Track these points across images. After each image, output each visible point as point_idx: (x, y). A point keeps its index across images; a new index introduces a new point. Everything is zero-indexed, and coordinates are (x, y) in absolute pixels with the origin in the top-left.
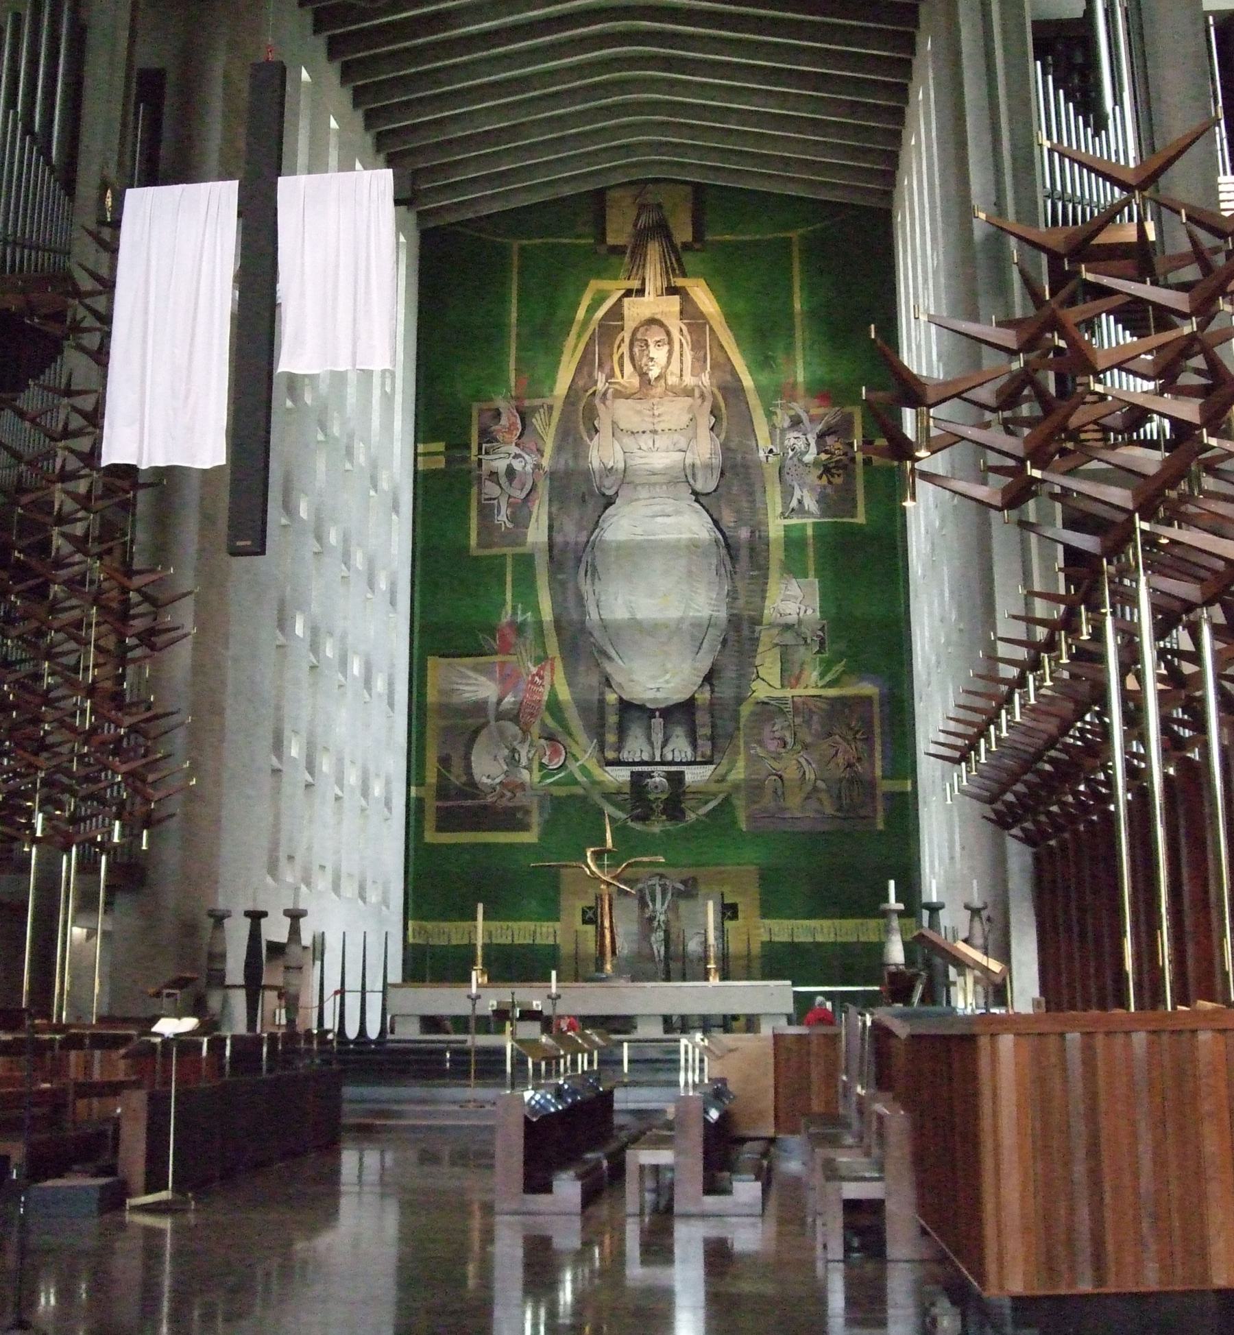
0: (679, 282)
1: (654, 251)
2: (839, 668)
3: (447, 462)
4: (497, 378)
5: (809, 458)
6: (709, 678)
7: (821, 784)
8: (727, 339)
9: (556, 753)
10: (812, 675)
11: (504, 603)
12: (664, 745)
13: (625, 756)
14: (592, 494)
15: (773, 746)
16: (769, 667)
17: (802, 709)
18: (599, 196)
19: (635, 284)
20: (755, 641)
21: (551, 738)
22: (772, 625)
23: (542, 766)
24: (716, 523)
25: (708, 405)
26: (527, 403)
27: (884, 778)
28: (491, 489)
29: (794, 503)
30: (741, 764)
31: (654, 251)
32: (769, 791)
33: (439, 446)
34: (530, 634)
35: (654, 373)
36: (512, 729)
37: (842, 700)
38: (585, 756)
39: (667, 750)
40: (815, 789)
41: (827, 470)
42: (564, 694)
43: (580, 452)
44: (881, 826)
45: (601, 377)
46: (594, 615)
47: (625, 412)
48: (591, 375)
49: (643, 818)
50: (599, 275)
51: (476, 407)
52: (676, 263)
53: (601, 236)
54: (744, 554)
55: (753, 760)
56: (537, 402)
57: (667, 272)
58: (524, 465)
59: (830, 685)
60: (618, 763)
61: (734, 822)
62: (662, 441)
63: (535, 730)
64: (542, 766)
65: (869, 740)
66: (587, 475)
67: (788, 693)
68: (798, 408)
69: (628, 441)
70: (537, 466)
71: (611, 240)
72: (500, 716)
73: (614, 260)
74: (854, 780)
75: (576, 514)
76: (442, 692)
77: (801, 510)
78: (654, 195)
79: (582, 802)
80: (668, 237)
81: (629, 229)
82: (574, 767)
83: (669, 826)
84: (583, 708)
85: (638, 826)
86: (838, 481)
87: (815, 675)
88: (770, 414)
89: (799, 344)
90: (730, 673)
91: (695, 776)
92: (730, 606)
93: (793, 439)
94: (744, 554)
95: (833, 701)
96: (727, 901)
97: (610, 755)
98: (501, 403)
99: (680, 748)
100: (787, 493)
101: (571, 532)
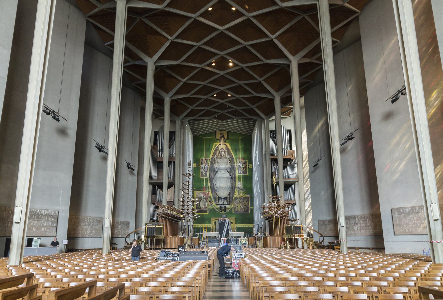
0: (226, 144)
1: (222, 139)
2: (245, 193)
3: (197, 166)
4: (202, 155)
5: (241, 167)
6: (229, 194)
7: (243, 207)
8: (231, 151)
9: (210, 203)
10: (242, 194)
11: (204, 184)
12: (224, 202)
13: (219, 204)
14: (215, 170)
15: (237, 202)
16: (236, 192)
17: (240, 198)
18: (216, 132)
19: (220, 144)
20: (235, 190)
21: (210, 201)
22: (237, 188)
23: (209, 205)
24: (230, 175)
25: (229, 160)
26: (207, 159)
27: (250, 207)
28: (202, 170)
29: (239, 172)
30: (233, 205)
31: (222, 139)
32: (236, 208)
33: (196, 164)
34: (207, 188)
35: (222, 155)
36: (205, 200)
37: (245, 197)
38: (214, 203)
39: (224, 203)
40: (242, 208)
41: (243, 168)
42: (211, 196)
43: (213, 165)
44: (250, 213)
45: (216, 156)
46: (215, 186)
47: (219, 160)
48: (214, 155)
49: (221, 211)
50: (216, 142)
51: (200, 159)
52: (225, 142)
53: (216, 137)
54: (233, 178)
55: (234, 205)
56: (208, 159)
57: (224, 142)
58: (206, 167)
59: (244, 195)
60: (218, 205)
61: (232, 212)
62: (223, 164)
63: (208, 200)
64: (209, 205)
65: (248, 202)
66: (214, 168)
67: (239, 196)
68: (240, 160)
69: (219, 164)
70: (208, 167)
71: (217, 138)
72: (203, 199)
73: (217, 140)
74: (247, 207)
75: (213, 173)
76: (196, 195)
77: (240, 173)
78: (222, 132)
79: (214, 209)
80: (224, 138)
81: (219, 136)
82: (213, 205)
83: (224, 212)
84: (214, 198)
85: (220, 212)
86: (245, 170)
87: (242, 194)
88: (237, 161)
89: (240, 152)
90: (232, 194)
91: (228, 206)
92: (232, 185)
93: (240, 165)
94: (233, 178)
95: (244, 197)
96: (231, 222)
97: (217, 204)
98: (203, 158)
99: (225, 203)
100: (239, 171)
101: (212, 176)
